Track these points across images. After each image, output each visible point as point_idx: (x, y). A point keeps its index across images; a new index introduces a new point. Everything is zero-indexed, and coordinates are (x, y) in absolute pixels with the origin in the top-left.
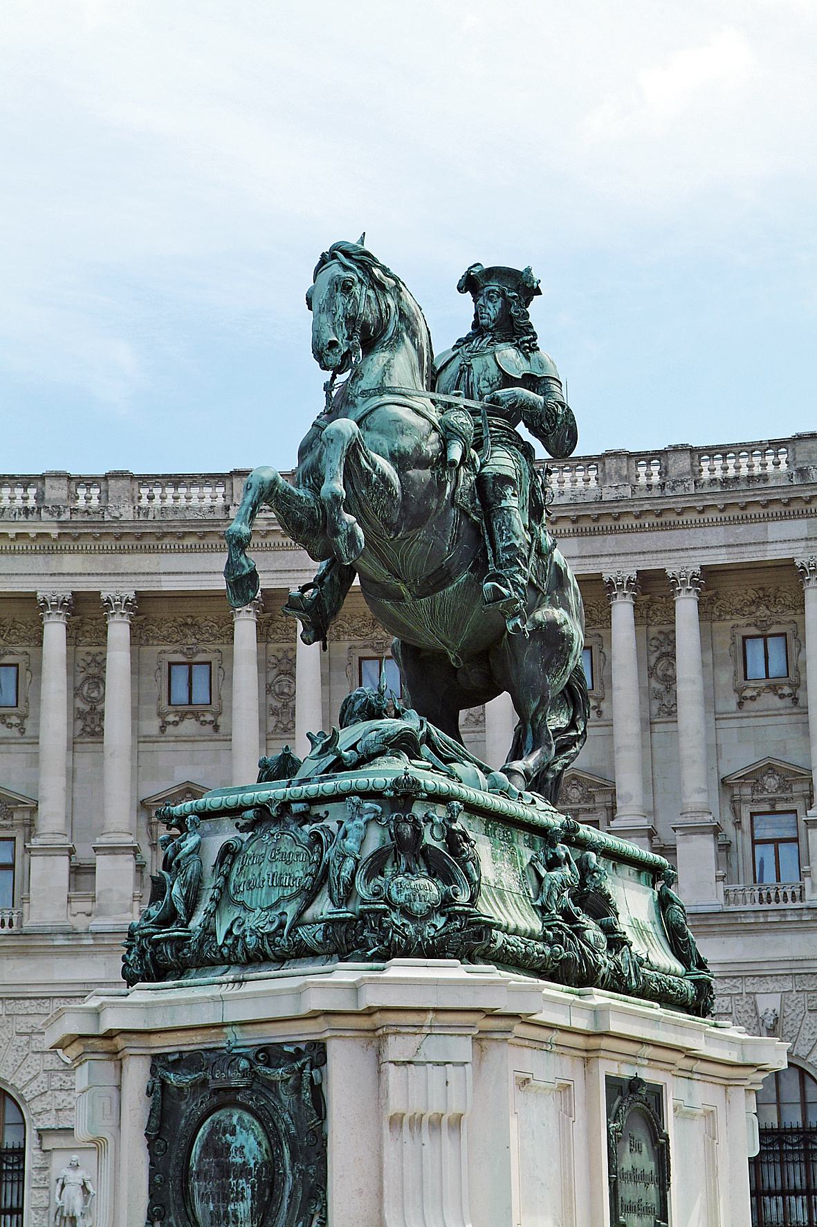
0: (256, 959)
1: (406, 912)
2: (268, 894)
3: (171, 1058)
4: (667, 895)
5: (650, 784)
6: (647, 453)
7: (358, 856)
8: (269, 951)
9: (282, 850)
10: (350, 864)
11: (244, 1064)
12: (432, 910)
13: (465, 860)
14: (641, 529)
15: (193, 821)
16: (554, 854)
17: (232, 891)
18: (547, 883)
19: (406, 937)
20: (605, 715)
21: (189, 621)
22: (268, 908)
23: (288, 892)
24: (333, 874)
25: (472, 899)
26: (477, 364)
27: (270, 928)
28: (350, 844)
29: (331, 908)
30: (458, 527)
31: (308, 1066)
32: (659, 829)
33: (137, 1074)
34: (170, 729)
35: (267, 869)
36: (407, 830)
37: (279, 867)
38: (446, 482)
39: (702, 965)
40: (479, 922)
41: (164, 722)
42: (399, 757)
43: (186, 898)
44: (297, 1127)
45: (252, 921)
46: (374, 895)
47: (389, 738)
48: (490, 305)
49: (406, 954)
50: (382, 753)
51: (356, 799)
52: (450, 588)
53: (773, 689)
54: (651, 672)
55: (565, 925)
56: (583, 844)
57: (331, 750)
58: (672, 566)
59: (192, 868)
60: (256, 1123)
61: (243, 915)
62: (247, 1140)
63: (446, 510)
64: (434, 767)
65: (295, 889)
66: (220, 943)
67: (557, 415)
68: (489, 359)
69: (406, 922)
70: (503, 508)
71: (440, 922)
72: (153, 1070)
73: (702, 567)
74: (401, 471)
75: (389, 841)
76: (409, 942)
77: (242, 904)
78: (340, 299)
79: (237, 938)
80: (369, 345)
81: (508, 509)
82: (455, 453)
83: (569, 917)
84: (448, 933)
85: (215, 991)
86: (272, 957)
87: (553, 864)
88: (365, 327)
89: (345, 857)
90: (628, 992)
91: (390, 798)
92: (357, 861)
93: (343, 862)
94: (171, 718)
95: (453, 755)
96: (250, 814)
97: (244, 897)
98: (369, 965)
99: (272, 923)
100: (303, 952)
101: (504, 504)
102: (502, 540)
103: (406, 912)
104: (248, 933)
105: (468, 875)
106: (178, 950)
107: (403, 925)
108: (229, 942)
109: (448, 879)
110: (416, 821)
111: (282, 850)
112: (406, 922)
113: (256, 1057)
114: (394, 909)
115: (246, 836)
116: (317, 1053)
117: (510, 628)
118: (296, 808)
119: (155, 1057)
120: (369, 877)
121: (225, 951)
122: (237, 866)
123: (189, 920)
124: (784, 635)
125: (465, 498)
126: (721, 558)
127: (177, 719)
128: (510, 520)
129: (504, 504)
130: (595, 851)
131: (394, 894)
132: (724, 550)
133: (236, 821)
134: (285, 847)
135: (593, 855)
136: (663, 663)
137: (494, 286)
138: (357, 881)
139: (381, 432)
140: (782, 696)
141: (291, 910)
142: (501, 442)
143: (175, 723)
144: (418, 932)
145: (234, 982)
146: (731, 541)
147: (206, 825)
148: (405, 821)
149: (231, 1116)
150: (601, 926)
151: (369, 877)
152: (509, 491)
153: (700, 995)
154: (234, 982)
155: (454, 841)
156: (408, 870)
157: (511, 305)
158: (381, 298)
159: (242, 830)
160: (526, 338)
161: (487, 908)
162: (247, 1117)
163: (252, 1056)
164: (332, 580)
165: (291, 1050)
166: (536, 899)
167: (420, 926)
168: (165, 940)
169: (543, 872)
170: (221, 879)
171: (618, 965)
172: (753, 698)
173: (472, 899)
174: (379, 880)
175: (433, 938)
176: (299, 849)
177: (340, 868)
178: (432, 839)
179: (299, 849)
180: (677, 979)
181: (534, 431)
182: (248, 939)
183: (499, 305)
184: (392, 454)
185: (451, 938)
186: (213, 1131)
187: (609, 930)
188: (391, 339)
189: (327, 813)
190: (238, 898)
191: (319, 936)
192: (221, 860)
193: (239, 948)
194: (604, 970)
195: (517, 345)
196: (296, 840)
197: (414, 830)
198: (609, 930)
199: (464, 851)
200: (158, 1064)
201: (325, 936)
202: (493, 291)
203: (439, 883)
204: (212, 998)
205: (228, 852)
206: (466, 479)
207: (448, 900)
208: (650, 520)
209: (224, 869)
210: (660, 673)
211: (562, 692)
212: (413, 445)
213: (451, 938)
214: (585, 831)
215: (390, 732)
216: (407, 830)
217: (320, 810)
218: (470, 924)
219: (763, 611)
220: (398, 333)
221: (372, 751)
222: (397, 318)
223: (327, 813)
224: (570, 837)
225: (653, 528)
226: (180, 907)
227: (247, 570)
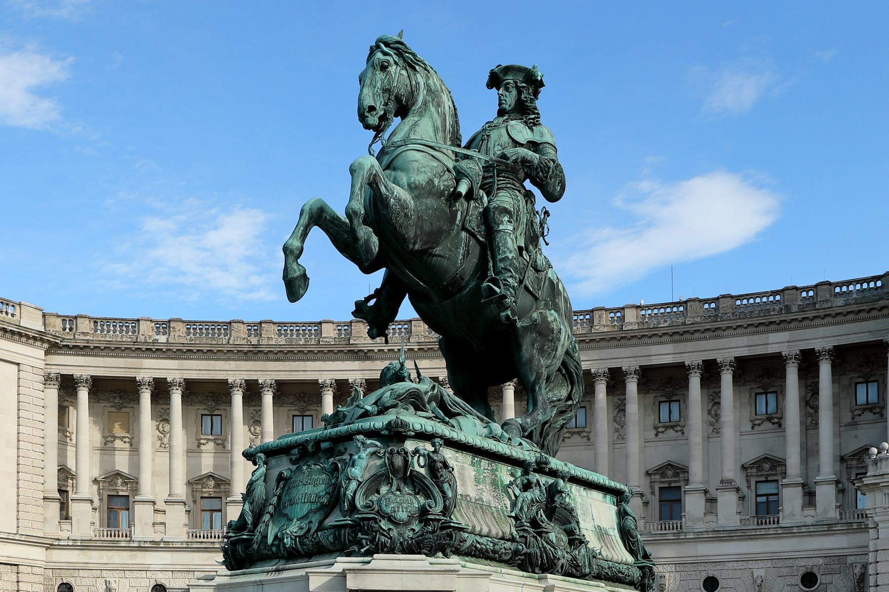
1: (391, 519)
4: (624, 510)
5: (707, 468)
6: (708, 300)
7: (360, 479)
13: (443, 482)
14: (705, 338)
19: (391, 538)
20: (686, 434)
25: (446, 511)
30: (467, 245)
32: (710, 490)
38: (457, 211)
39: (646, 556)
40: (450, 527)
42: (407, 409)
49: (392, 551)
53: (769, 419)
54: (709, 413)
55: (531, 530)
56: (553, 473)
58: (719, 357)
63: (458, 234)
64: (436, 417)
67: (549, 168)
69: (391, 527)
71: (416, 526)
73: (735, 358)
74: (416, 198)
76: (393, 542)
81: (503, 231)
82: (463, 189)
83: (534, 523)
85: (263, 577)
90: (583, 576)
91: (387, 436)
93: (349, 483)
95: (457, 410)
98: (361, 559)
101: (501, 227)
103: (391, 519)
107: (389, 529)
109: (428, 495)
110: (406, 453)
112: (391, 527)
114: (383, 518)
124: (776, 392)
125: (474, 224)
126: (745, 352)
129: (501, 227)
130: (563, 478)
131: (384, 508)
132: (746, 349)
135: (561, 481)
136: (715, 408)
138: (357, 497)
140: (773, 423)
144: (400, 535)
146: (750, 344)
148: (398, 453)
150: (565, 530)
152: (506, 219)
153: (643, 577)
155: (436, 468)
156: (399, 489)
161: (459, 518)
166: (511, 512)
167: (402, 529)
171: (574, 558)
172: (759, 425)
173: (446, 511)
174: (375, 497)
175: (412, 538)
178: (419, 467)
180: (625, 567)
181: (534, 182)
184: (409, 185)
185: (426, 539)
187: (570, 533)
194: (562, 561)
198: (570, 533)
199: (442, 476)
204: (255, 582)
206: (475, 209)
207: (423, 512)
208: (708, 335)
210: (713, 413)
211: (559, 370)
212: (427, 179)
214: (555, 463)
216: (398, 461)
218: (442, 528)
219: (766, 380)
224: (541, 468)
225: (711, 338)
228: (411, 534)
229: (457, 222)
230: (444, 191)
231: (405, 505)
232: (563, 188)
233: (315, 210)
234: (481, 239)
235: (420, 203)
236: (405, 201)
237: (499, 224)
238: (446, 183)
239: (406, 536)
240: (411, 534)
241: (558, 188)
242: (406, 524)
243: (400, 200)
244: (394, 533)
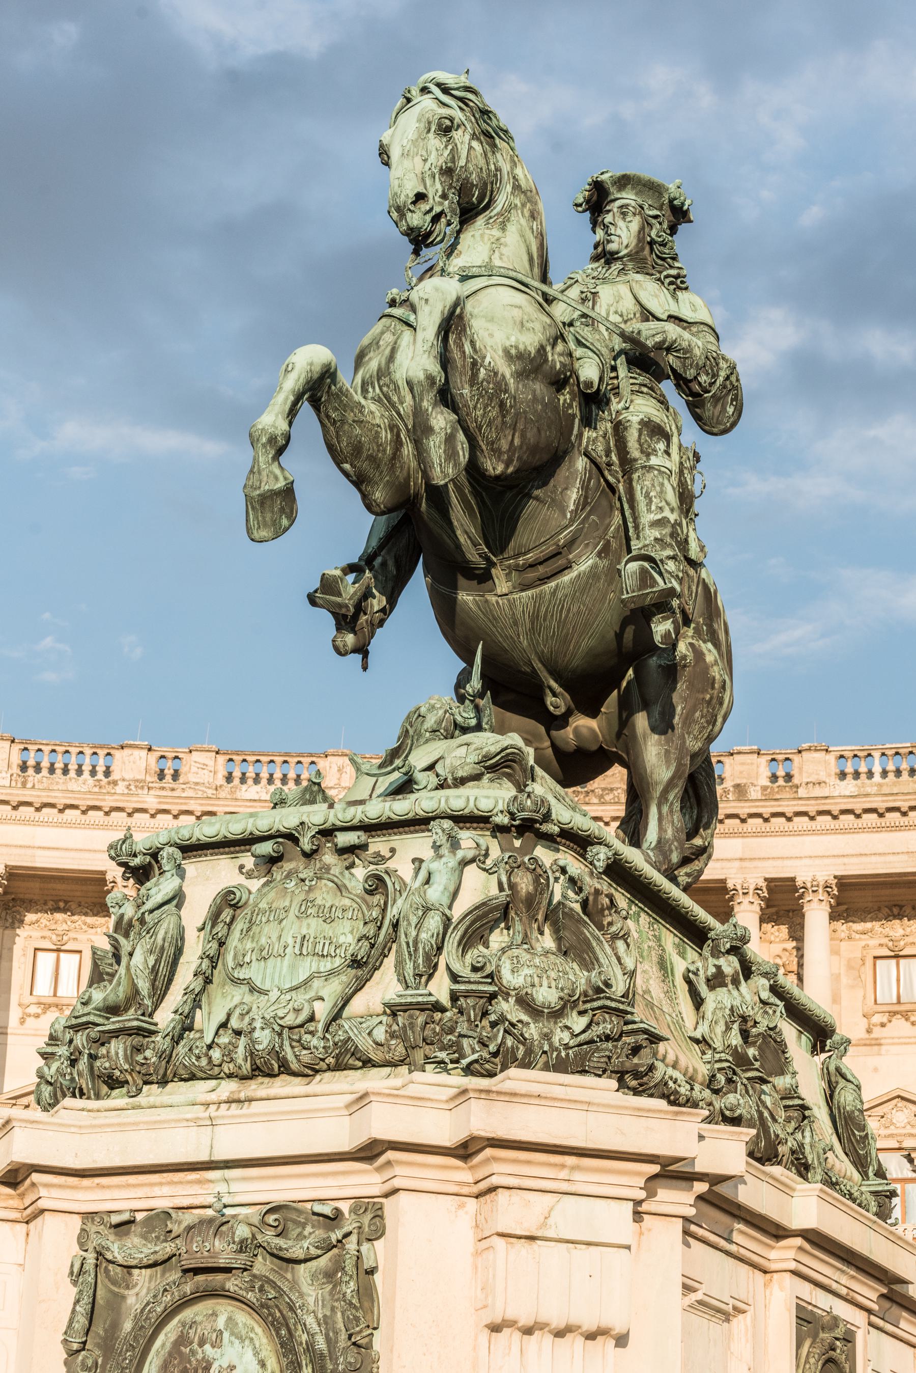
0: (267, 1067)
1: (525, 1002)
2: (293, 967)
3: (115, 1219)
8: (290, 1057)
9: (319, 901)
10: (434, 923)
11: (243, 1232)
12: (568, 1004)
15: (171, 857)
16: (718, 968)
17: (231, 964)
18: (709, 1006)
21: (62, 905)
22: (292, 989)
23: (326, 965)
24: (408, 932)
26: (606, 293)
27: (290, 1020)
28: (436, 894)
29: (399, 988)
30: (585, 487)
31: (354, 1238)
33: (59, 1241)
34: (30, 1021)
35: (292, 929)
36: (525, 883)
37: (313, 927)
41: (24, 1013)
43: (154, 970)
44: (328, 1340)
45: (261, 1008)
46: (475, 969)
47: (487, 757)
48: (621, 223)
50: (477, 777)
51: (447, 824)
52: (566, 578)
57: (398, 762)
59: (165, 929)
60: (259, 1330)
61: (248, 998)
62: (241, 1356)
65: (338, 961)
66: (208, 1040)
68: (624, 290)
70: (651, 468)
71: (578, 1023)
72: (83, 1239)
75: (494, 891)
77: (248, 982)
78: (435, 142)
79: (238, 1033)
80: (469, 212)
84: (591, 1042)
86: (294, 1066)
87: (717, 981)
88: (464, 189)
89: (427, 909)
92: (447, 921)
94: (33, 1009)
96: (266, 848)
97: (254, 972)
99: (297, 1011)
100: (348, 1058)
101: (654, 461)
102: (649, 510)
103: (525, 1002)
104: (258, 1024)
105: (619, 959)
106: (138, 1049)
108: (224, 1039)
109: (588, 960)
111: (319, 901)
112: (525, 1018)
113: (263, 1221)
115: (255, 885)
116: (373, 1217)
117: (657, 638)
118: (343, 839)
119: (89, 1216)
120: (466, 944)
121: (216, 1054)
122: (239, 925)
123: (156, 1007)
127: (39, 1011)
128: (662, 485)
129: (654, 461)
133: (239, 862)
134: (324, 895)
137: (628, 197)
139: (491, 320)
141: (332, 990)
142: (642, 393)
143: (37, 1016)
145: (229, 1102)
147: (192, 867)
149: (215, 1314)
151: (466, 944)
154: (229, 1102)
157: (651, 226)
158: (489, 154)
159: (249, 875)
160: (673, 272)
162: (243, 1318)
163: (256, 1220)
164: (384, 564)
165: (327, 1210)
168: (116, 1034)
169: (703, 989)
170: (215, 945)
175: (567, 1047)
176: (347, 902)
177: (419, 926)
179: (347, 902)
182: (257, 1034)
183: (635, 224)
184: (507, 352)
186: (182, 1340)
188: (500, 214)
189: (393, 851)
190: (241, 974)
191: (380, 1034)
192: (215, 917)
193: (241, 1050)
195: (659, 280)
196: (340, 888)
197: (536, 881)
200: (92, 1228)
201: (392, 1035)
202: (626, 206)
203: (575, 966)
205: (229, 903)
209: (220, 929)
212: (536, 344)
213: (598, 1049)
215: (494, 749)
217: (378, 845)
220: (510, 208)
221: (460, 773)
222: (509, 188)
223: (393, 851)
226: (144, 985)
227: (281, 484)
228: (566, 1037)
229: (573, 438)
230: (559, 373)
231: (553, 974)
232: (739, 411)
233: (317, 369)
234: (610, 478)
235: (524, 386)
236: (503, 376)
237: (648, 455)
238: (562, 359)
239: (556, 1040)
240: (566, 1037)
241: (730, 410)
242: (557, 1014)
243: (496, 374)
244: (533, 1031)
